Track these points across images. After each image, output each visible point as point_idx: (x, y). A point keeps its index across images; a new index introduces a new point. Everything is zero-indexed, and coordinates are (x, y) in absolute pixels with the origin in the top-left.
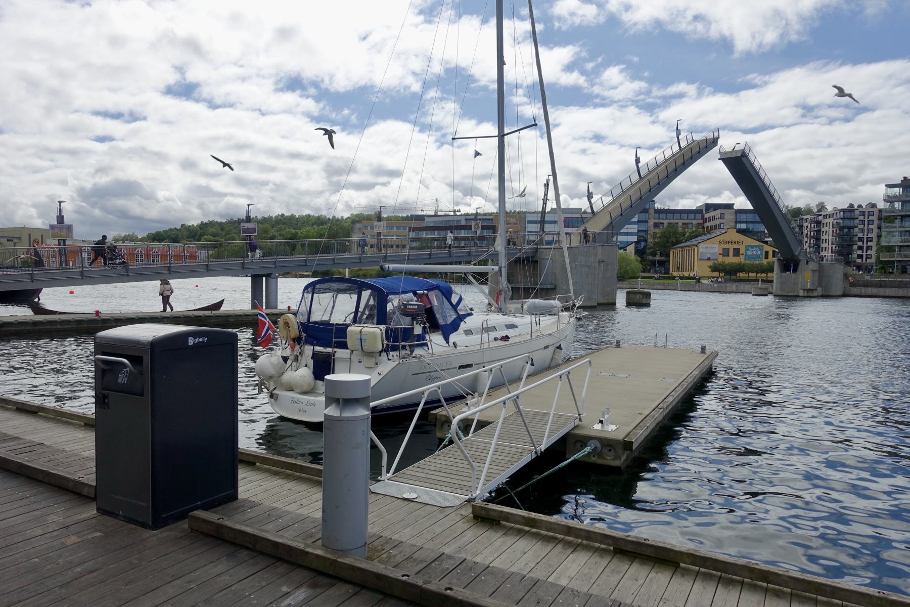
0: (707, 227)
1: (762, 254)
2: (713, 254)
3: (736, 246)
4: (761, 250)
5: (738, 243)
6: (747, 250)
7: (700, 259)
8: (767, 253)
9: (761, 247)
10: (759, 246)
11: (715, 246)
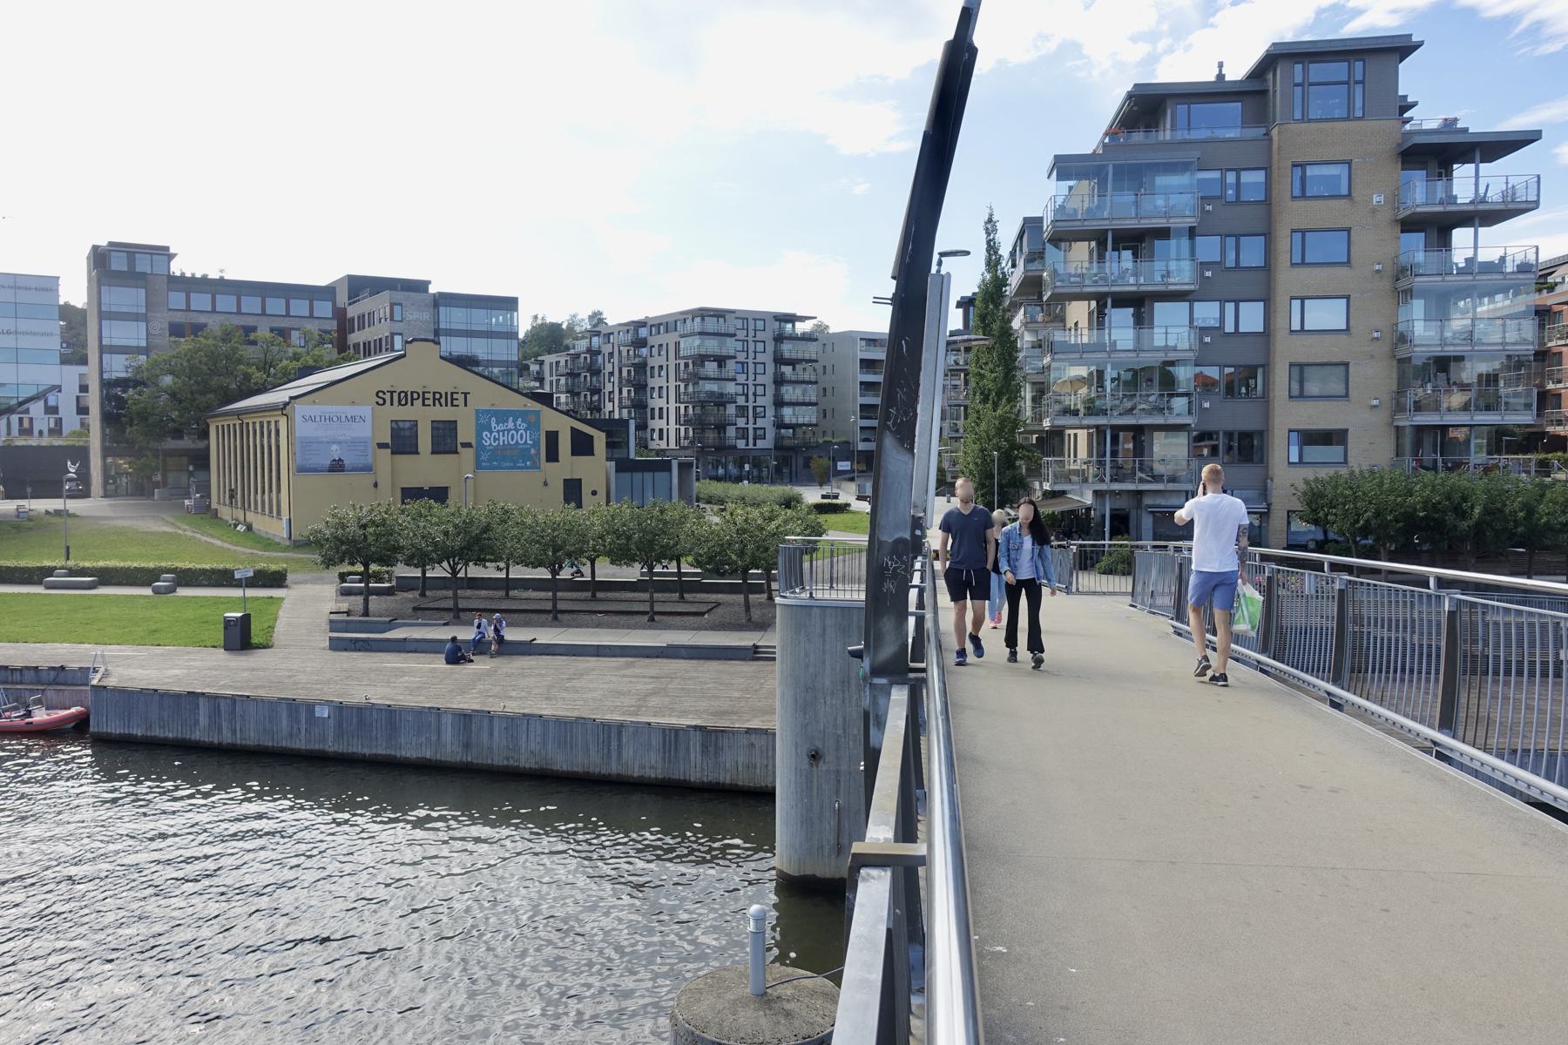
0: (356, 346)
1: (536, 444)
2: (355, 442)
3: (443, 413)
4: (533, 425)
5: (450, 399)
6: (482, 428)
7: (302, 470)
8: (552, 438)
9: (532, 418)
10: (523, 415)
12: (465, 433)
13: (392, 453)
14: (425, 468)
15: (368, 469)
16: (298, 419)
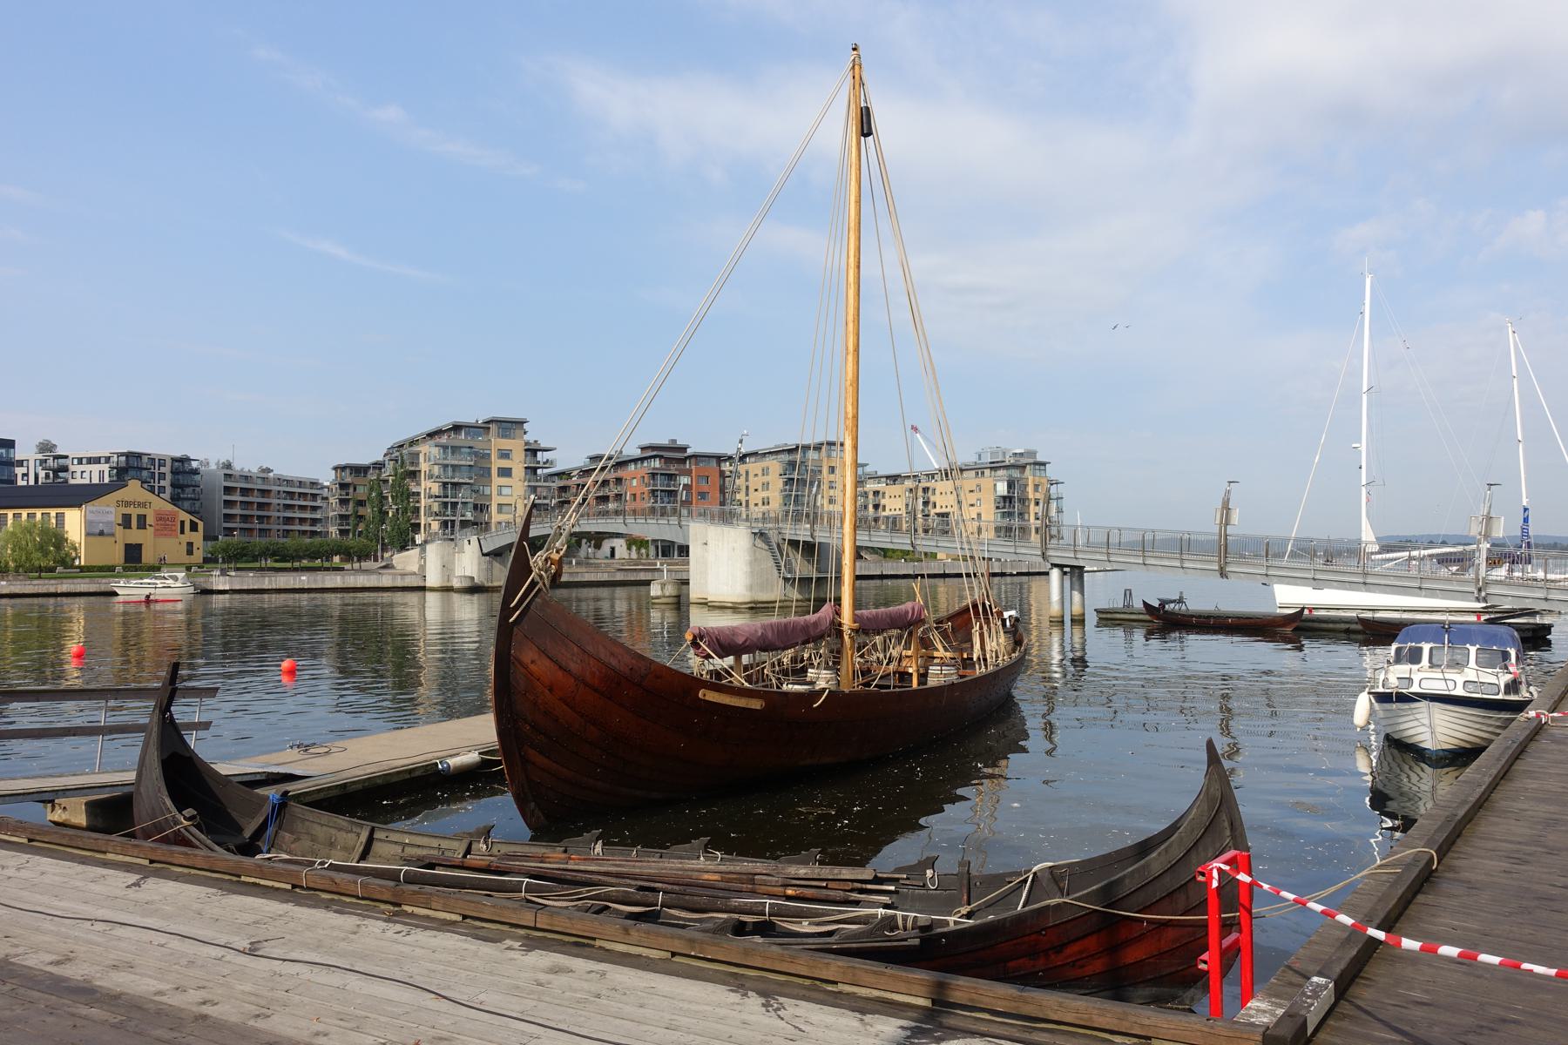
2: (108, 523)
3: (141, 511)
5: (143, 505)
8: (182, 523)
11: (108, 509)
12: (150, 520)
14: (135, 536)
15: (113, 535)
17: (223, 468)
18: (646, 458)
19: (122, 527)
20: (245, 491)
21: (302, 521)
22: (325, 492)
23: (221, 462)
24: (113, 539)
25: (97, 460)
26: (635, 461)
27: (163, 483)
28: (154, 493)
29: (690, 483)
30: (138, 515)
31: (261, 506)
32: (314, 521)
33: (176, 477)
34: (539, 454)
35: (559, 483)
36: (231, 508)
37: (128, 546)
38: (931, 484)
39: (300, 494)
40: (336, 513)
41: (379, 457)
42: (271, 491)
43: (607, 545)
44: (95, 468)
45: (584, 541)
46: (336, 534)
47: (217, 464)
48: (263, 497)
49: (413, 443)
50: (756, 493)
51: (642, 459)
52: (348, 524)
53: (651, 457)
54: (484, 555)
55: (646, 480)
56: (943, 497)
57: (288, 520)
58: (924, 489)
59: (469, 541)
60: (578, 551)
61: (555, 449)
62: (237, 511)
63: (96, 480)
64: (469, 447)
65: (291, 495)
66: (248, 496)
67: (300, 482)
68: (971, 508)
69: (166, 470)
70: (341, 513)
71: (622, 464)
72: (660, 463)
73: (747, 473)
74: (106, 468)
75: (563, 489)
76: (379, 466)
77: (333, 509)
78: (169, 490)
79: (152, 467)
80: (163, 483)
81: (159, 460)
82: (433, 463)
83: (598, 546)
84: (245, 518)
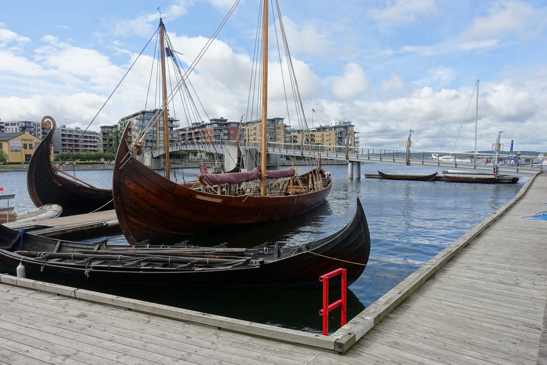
2: (19, 147)
3: (30, 143)
7: (11, 151)
13: (24, 149)
15: (20, 151)
16: (10, 143)
17: (62, 127)
18: (212, 124)
19: (23, 148)
20: (70, 136)
21: (91, 146)
22: (98, 136)
23: (61, 125)
24: (20, 153)
25: (14, 124)
26: (208, 125)
27: (39, 133)
28: (36, 137)
29: (228, 133)
30: (29, 144)
31: (76, 141)
32: (94, 146)
33: (44, 130)
34: (174, 122)
35: (181, 133)
36: (64, 142)
37: (26, 155)
38: (314, 133)
39: (89, 137)
40: (102, 143)
41: (115, 123)
42: (78, 135)
43: (199, 155)
44: (14, 127)
45: (190, 153)
46: (102, 151)
47: (60, 126)
48: (76, 138)
49: (128, 118)
50: (252, 136)
51: (211, 124)
52: (106, 148)
53: (214, 123)
54: (154, 158)
55: (212, 132)
56: (318, 137)
57: (86, 146)
58: (311, 135)
59: (148, 153)
60: (189, 157)
61: (179, 120)
62: (67, 143)
63: (14, 132)
64: (148, 120)
65: (86, 137)
66: (70, 137)
67: (89, 132)
68: (327, 142)
69: (40, 128)
70: (104, 143)
71: (204, 126)
72: (217, 125)
73: (248, 129)
74: (18, 127)
75: (183, 135)
76: (116, 126)
77: (101, 142)
78: (41, 135)
79: (35, 127)
80: (39, 133)
81: (37, 124)
82: (135, 125)
83: (195, 155)
84: (70, 145)
